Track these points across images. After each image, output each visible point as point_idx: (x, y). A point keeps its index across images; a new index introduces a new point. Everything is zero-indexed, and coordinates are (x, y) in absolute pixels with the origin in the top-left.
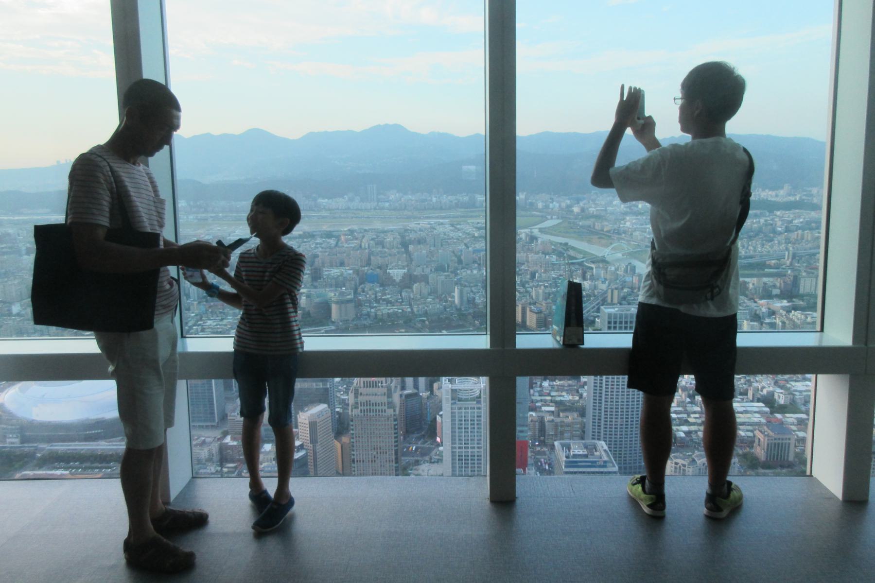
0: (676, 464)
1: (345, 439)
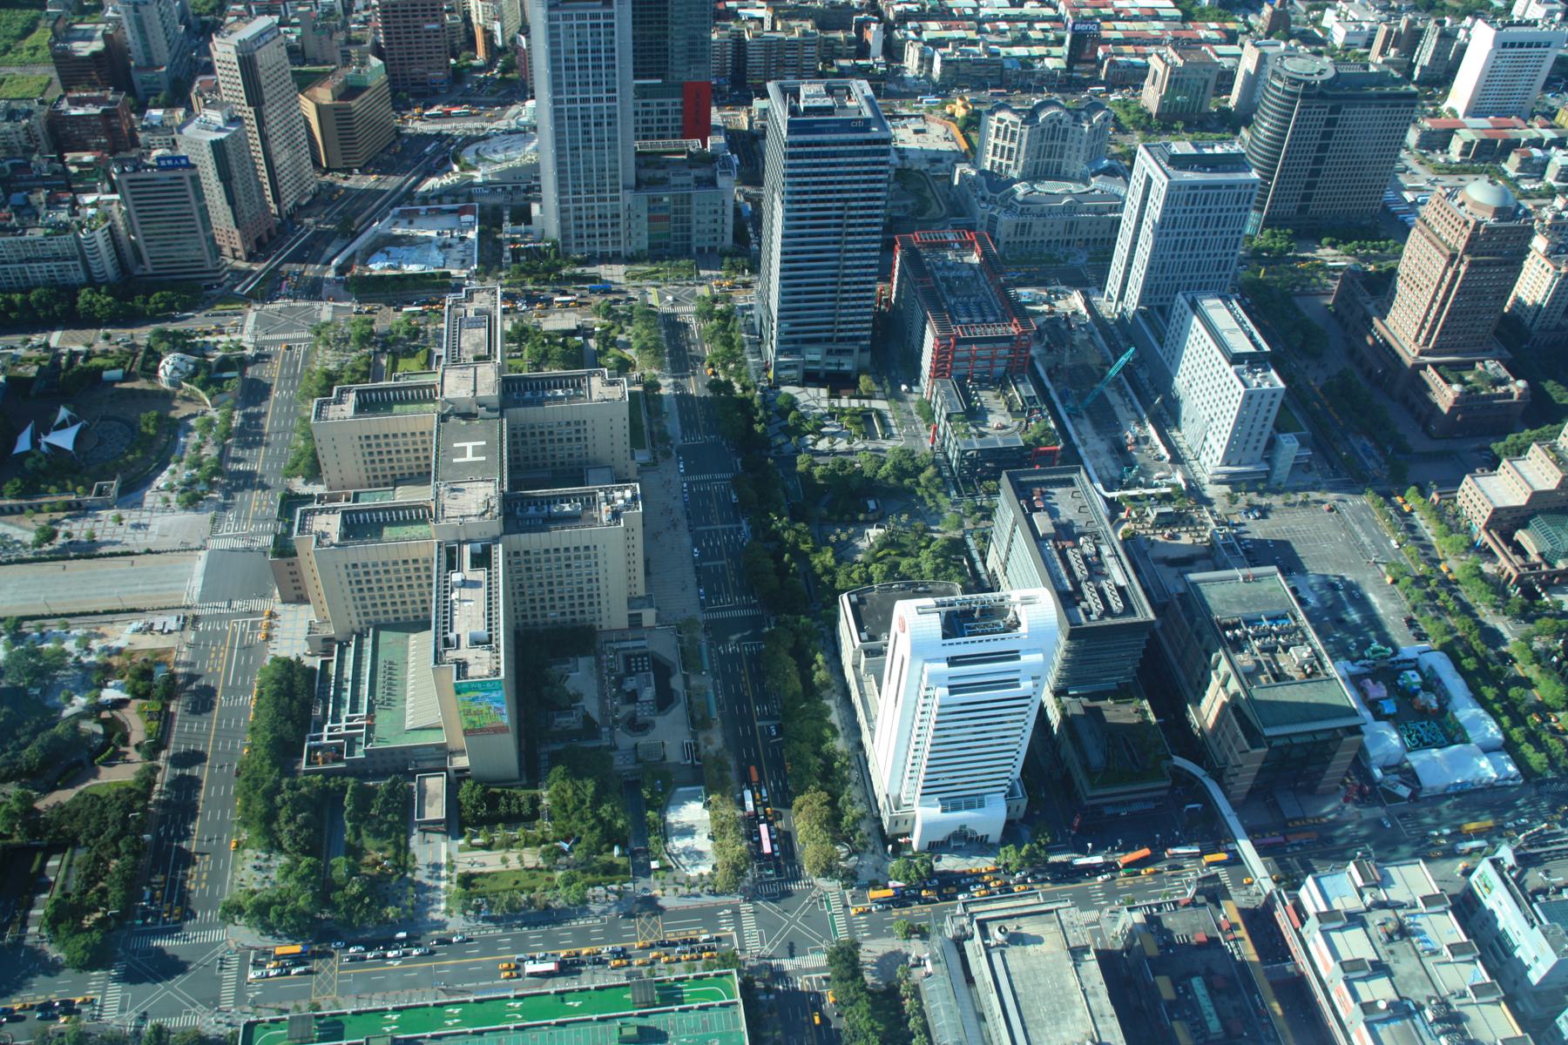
0: (1000, 121)
1: (325, 95)
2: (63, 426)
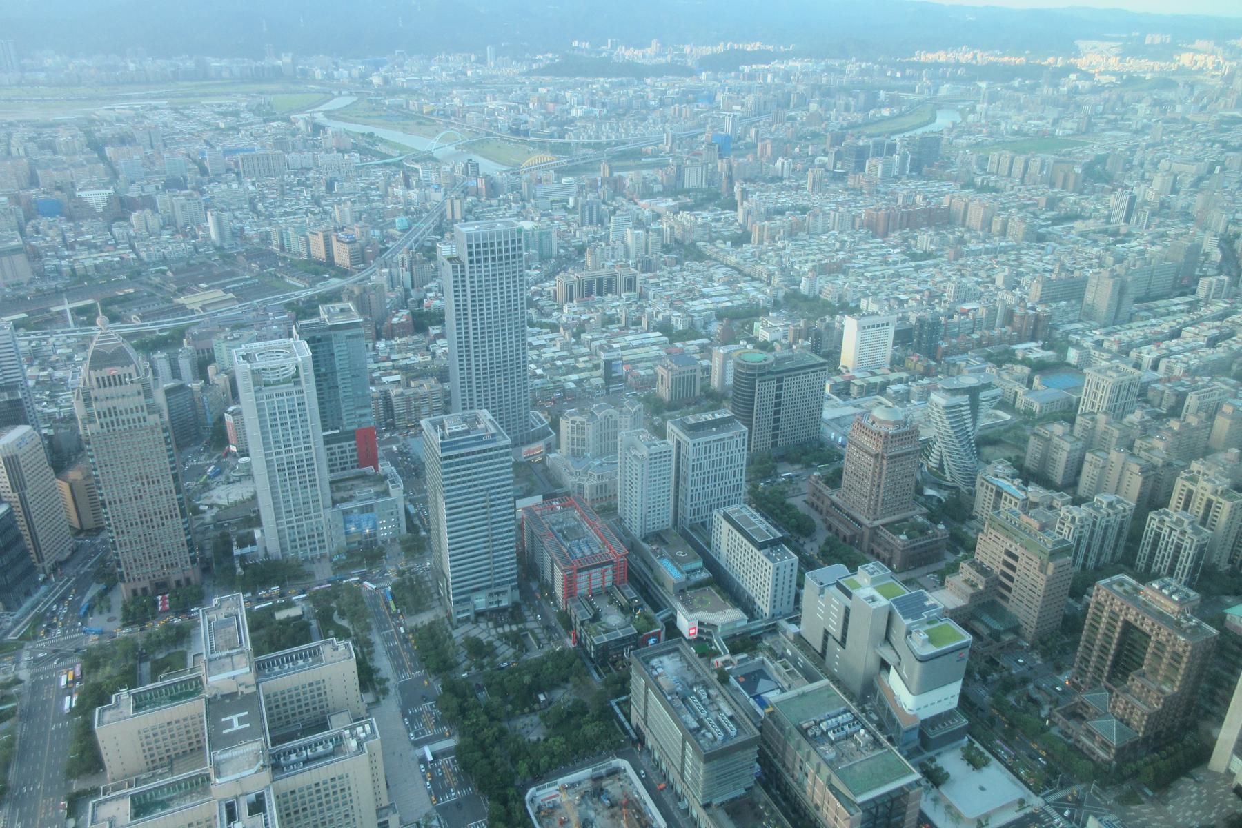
0: (573, 422)
1: (74, 474)
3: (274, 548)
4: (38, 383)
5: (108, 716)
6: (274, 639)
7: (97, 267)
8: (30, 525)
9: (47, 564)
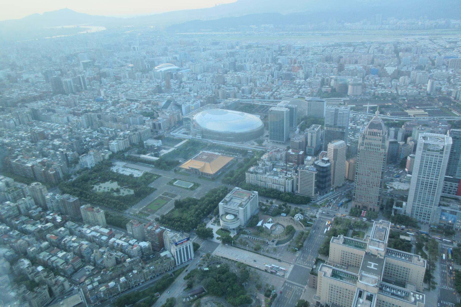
1: (352, 161)
2: (269, 223)
3: (409, 212)
4: (351, 128)
5: (335, 240)
6: (396, 244)
7: (382, 94)
8: (334, 172)
9: (335, 186)
